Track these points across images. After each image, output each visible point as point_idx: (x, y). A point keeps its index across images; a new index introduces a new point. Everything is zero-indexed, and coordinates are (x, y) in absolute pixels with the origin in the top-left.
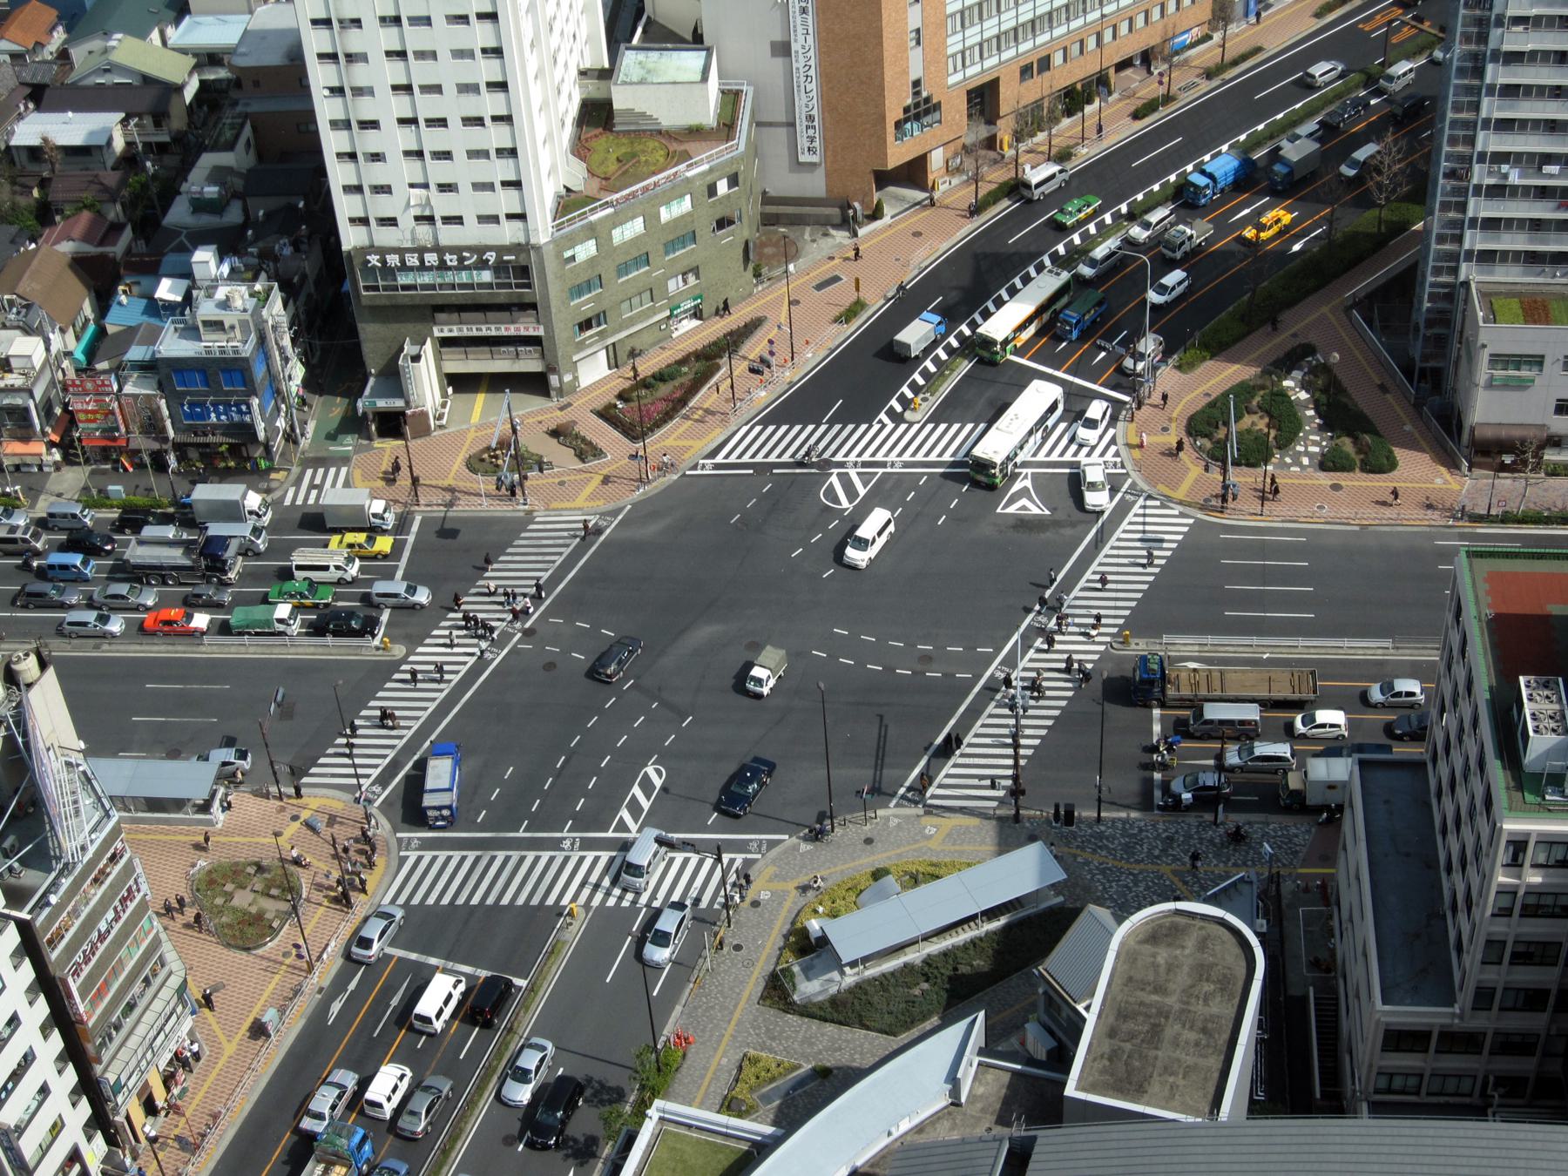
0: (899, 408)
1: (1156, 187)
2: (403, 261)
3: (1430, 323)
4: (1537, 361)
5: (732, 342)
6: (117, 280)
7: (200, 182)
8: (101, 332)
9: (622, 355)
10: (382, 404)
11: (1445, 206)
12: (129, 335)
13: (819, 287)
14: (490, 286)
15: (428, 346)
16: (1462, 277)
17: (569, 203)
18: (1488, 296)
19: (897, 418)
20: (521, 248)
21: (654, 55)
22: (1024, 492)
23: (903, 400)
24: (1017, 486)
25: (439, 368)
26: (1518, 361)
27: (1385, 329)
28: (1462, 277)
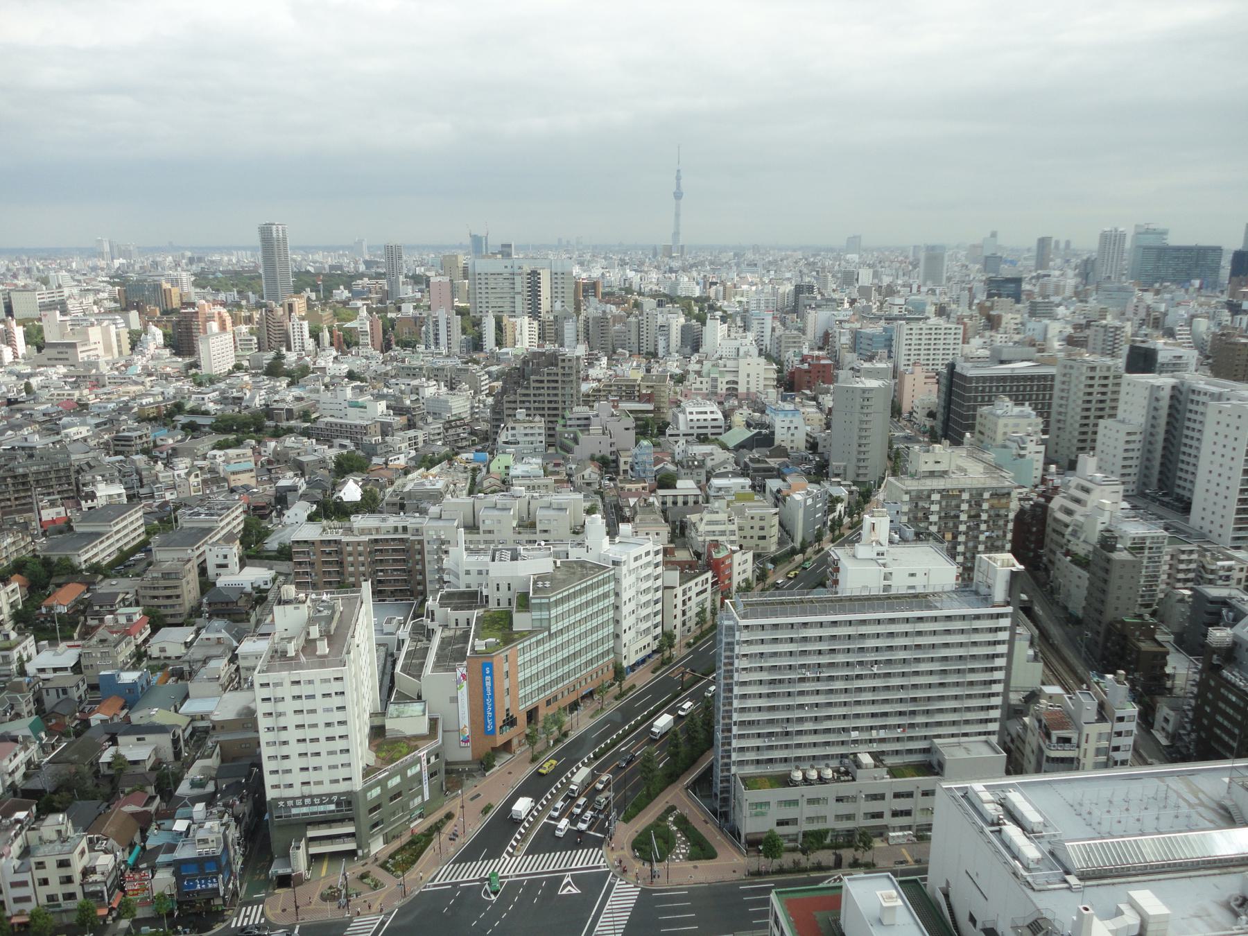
0: (511, 851)
2: (294, 803)
3: (722, 792)
4: (768, 804)
5: (437, 828)
6: (151, 821)
7: (194, 772)
8: (143, 848)
9: (390, 838)
10: (281, 871)
11: (723, 744)
12: (157, 850)
13: (472, 799)
14: (333, 811)
15: (303, 842)
16: (733, 772)
17: (368, 771)
18: (744, 779)
19: (511, 855)
20: (350, 793)
21: (402, 705)
22: (568, 884)
23: (512, 846)
24: (565, 882)
25: (307, 851)
26: (762, 804)
28: (733, 772)
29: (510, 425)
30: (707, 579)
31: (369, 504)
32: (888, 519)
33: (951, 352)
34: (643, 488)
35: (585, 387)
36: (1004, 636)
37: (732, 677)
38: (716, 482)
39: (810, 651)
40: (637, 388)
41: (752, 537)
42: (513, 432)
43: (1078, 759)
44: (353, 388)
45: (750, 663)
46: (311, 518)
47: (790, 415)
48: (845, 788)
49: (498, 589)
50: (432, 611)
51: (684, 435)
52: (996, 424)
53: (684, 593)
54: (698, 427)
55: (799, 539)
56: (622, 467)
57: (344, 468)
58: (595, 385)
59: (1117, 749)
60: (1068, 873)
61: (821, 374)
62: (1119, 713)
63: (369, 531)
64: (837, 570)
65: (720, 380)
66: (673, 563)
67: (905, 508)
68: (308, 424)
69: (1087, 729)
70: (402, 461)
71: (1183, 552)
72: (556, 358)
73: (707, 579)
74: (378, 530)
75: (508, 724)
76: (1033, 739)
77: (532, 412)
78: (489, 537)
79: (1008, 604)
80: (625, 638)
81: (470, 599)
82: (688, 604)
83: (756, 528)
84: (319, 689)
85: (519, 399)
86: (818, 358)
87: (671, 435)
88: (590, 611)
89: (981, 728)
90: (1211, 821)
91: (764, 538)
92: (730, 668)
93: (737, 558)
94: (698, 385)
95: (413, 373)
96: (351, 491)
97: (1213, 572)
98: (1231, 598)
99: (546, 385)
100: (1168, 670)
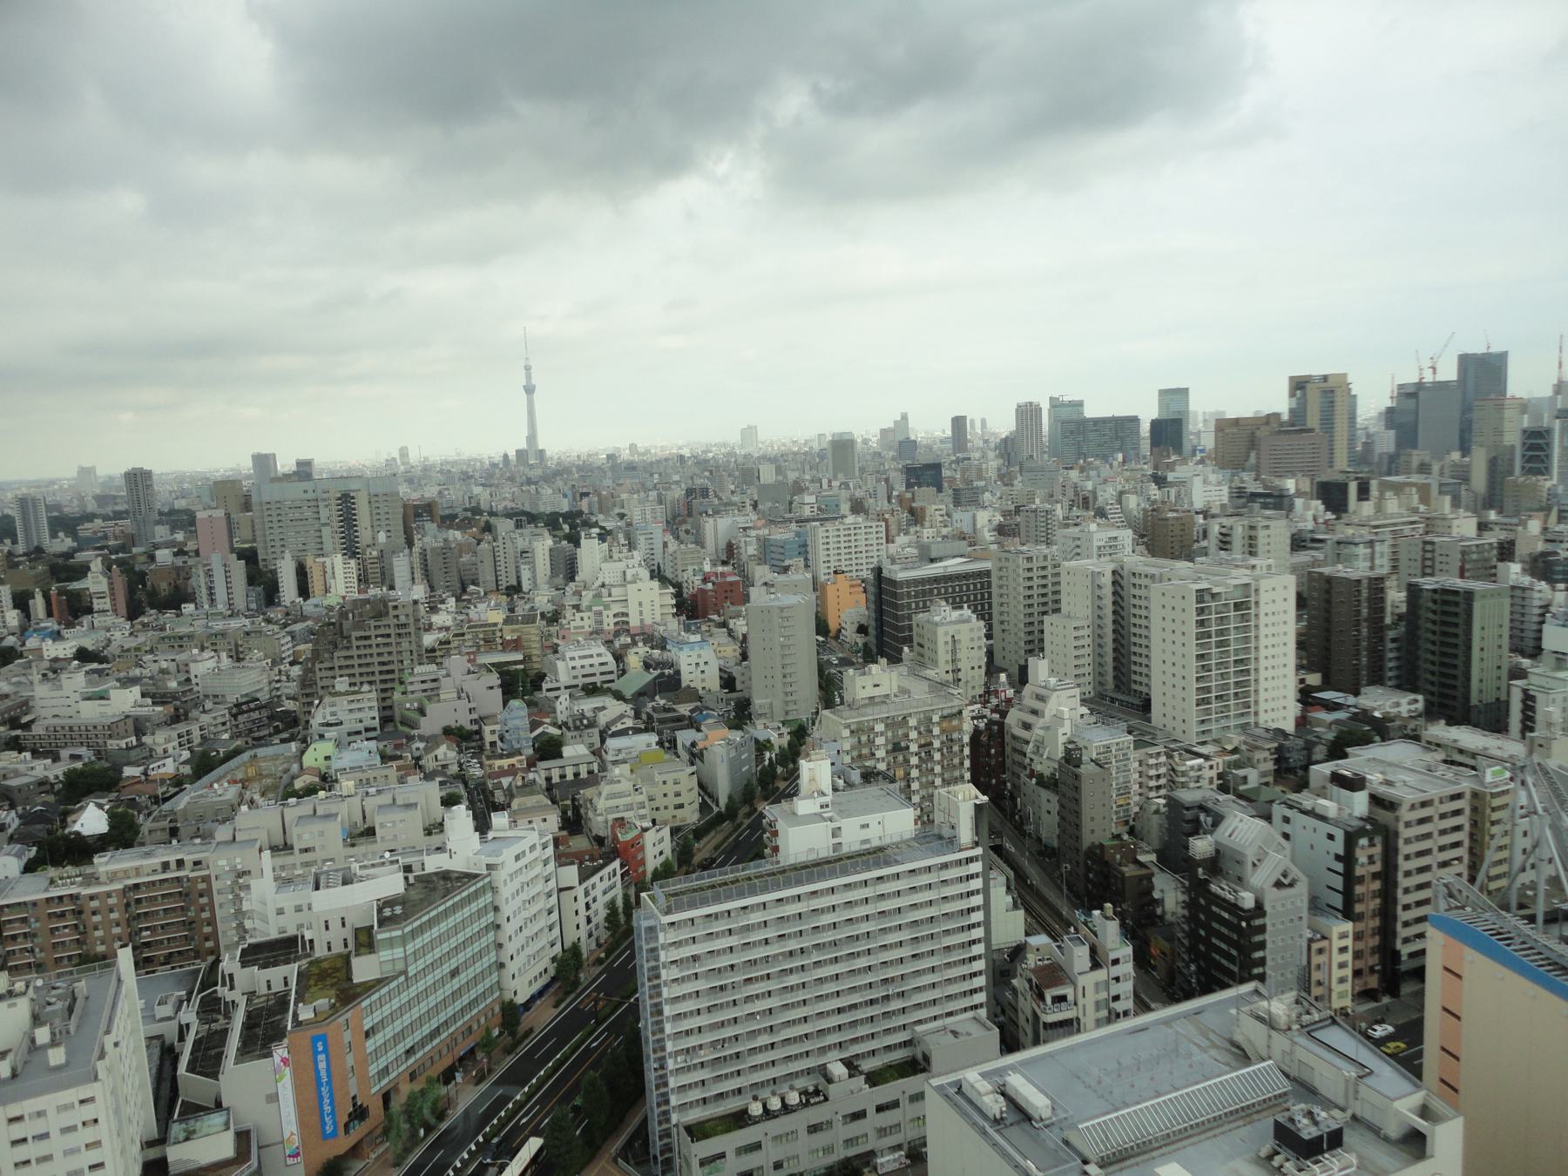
1: (495, 1121)
3: (662, 1153)
4: (722, 1156)
11: (658, 1087)
21: (192, 1122)
27: (637, 1164)
29: (327, 699)
30: (614, 870)
31: (122, 835)
32: (829, 762)
33: (875, 554)
34: (520, 761)
35: (429, 640)
36: (977, 884)
37: (659, 994)
38: (612, 743)
39: (754, 943)
40: (499, 634)
41: (666, 808)
42: (333, 709)
43: (1078, 1019)
44: (87, 672)
45: (681, 971)
46: (29, 868)
47: (697, 648)
48: (815, 1115)
49: (327, 928)
50: (231, 976)
51: (566, 688)
52: (935, 633)
53: (587, 894)
54: (584, 676)
55: (723, 801)
56: (488, 738)
57: (78, 788)
58: (442, 635)
59: (1116, 998)
60: (1085, 1162)
61: (729, 594)
62: (1112, 956)
63: (126, 874)
64: (775, 834)
65: (605, 613)
66: (567, 855)
67: (847, 746)
68: (18, 732)
69: (1082, 981)
70: (169, 768)
71: (1151, 756)
72: (386, 606)
73: (614, 870)
74: (138, 871)
75: (356, 1118)
76: (1026, 1004)
77: (358, 679)
78: (308, 857)
79: (977, 844)
80: (512, 967)
81: (282, 949)
82: (593, 906)
83: (671, 795)
84: (54, 1123)
85: (337, 663)
86: (723, 575)
87: (548, 690)
88: (461, 937)
89: (967, 1002)
90: (1227, 1064)
91: (681, 806)
92: (656, 982)
93: (650, 837)
94: (578, 623)
95: (179, 642)
96: (92, 820)
97: (1184, 774)
98: (1206, 801)
99: (373, 642)
100: (1156, 895)
